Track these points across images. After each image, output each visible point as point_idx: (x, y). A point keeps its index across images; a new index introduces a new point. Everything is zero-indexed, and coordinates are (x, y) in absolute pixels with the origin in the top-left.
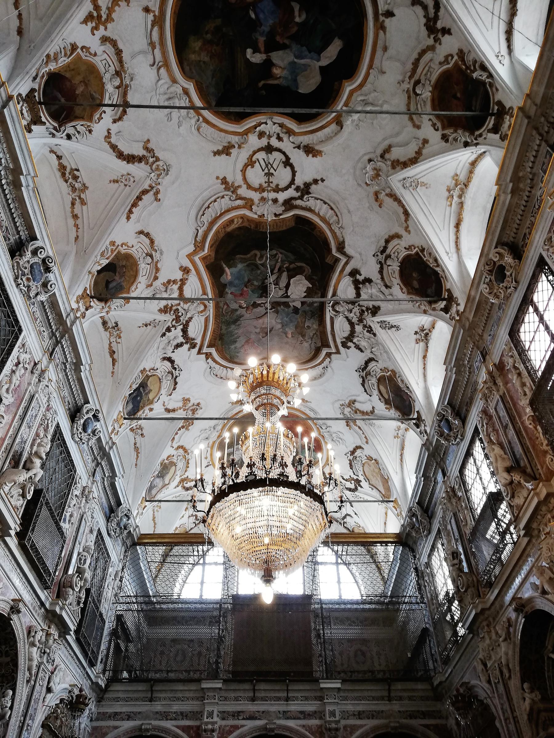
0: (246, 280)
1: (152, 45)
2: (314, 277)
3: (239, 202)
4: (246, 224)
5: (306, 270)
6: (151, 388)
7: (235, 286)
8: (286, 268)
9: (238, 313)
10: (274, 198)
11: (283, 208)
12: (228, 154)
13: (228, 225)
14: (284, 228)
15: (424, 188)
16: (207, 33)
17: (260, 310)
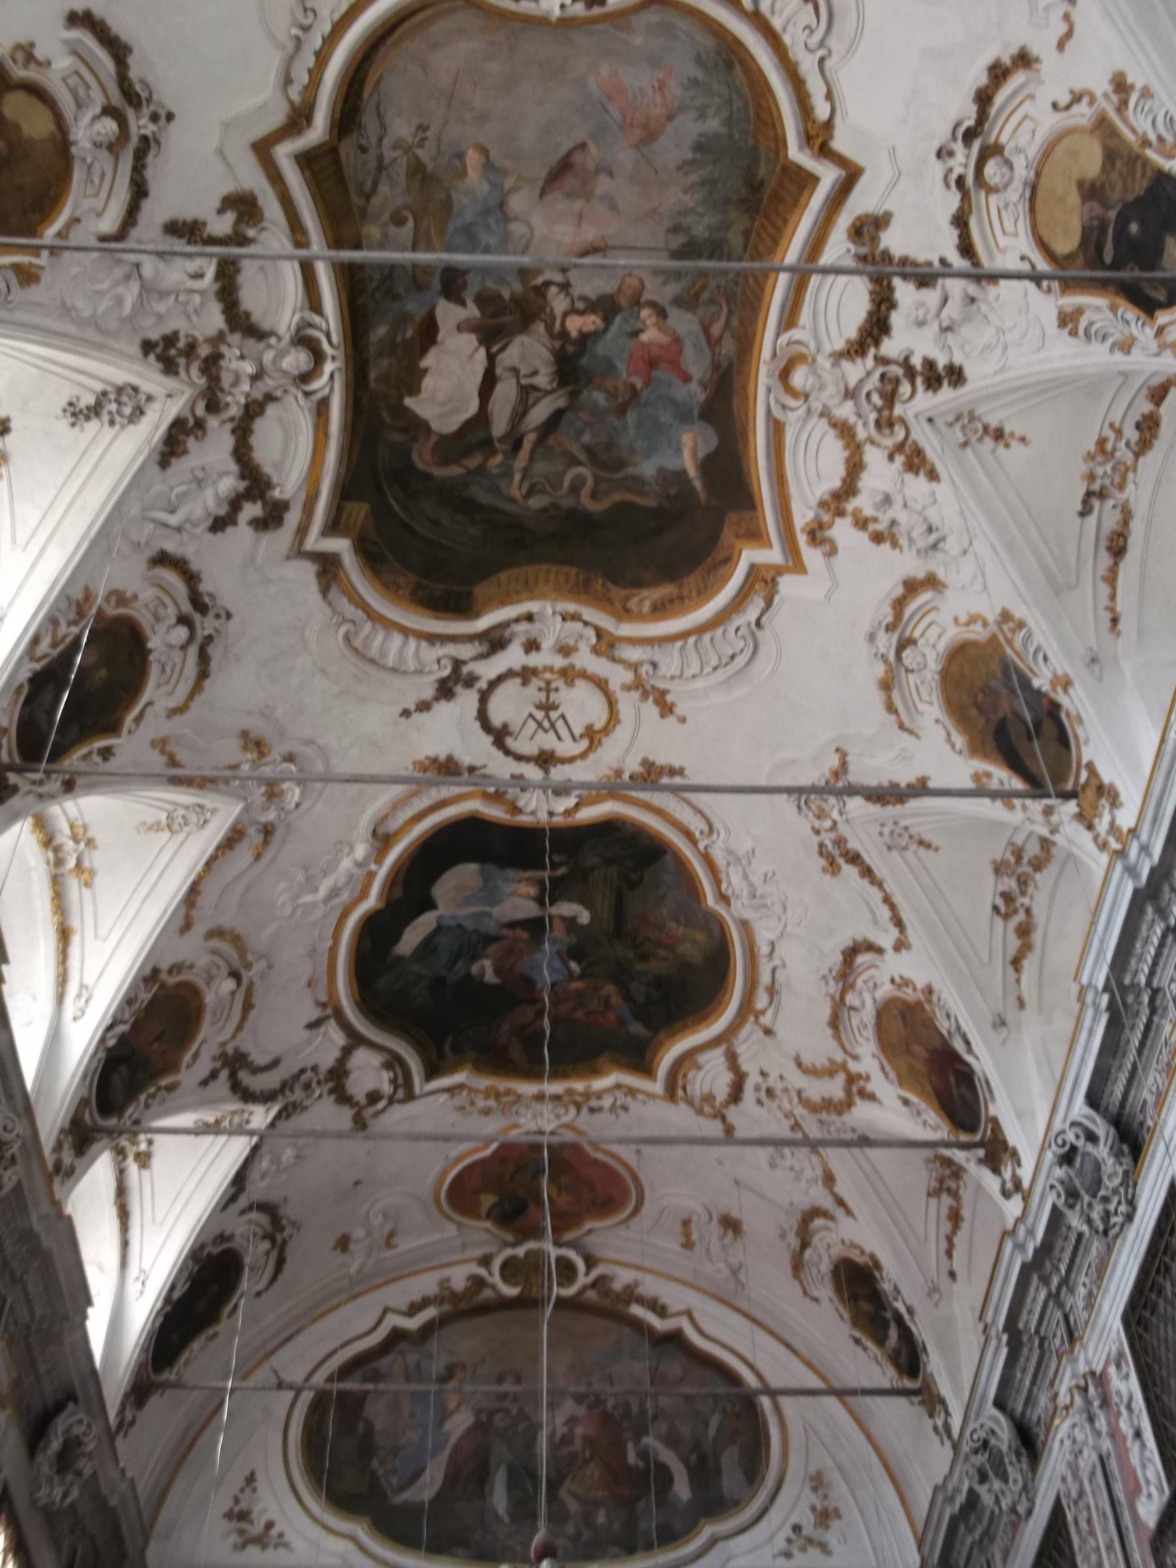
0: (631, 417)
1: (772, 991)
2: (397, 437)
3: (633, 654)
4: (617, 593)
5: (428, 457)
6: (1074, 198)
7: (673, 401)
8: (494, 452)
9: (673, 289)
10: (534, 654)
11: (507, 633)
12: (648, 764)
13: (671, 601)
14: (503, 576)
15: (150, 820)
16: (666, 959)
17: (591, 286)
